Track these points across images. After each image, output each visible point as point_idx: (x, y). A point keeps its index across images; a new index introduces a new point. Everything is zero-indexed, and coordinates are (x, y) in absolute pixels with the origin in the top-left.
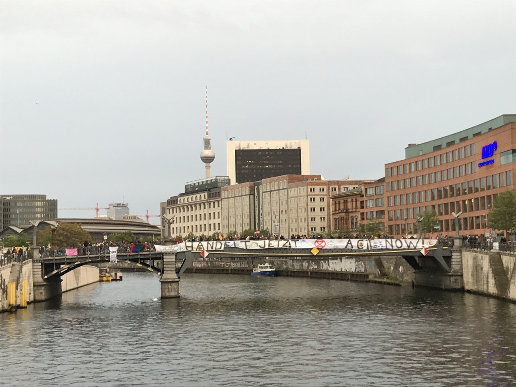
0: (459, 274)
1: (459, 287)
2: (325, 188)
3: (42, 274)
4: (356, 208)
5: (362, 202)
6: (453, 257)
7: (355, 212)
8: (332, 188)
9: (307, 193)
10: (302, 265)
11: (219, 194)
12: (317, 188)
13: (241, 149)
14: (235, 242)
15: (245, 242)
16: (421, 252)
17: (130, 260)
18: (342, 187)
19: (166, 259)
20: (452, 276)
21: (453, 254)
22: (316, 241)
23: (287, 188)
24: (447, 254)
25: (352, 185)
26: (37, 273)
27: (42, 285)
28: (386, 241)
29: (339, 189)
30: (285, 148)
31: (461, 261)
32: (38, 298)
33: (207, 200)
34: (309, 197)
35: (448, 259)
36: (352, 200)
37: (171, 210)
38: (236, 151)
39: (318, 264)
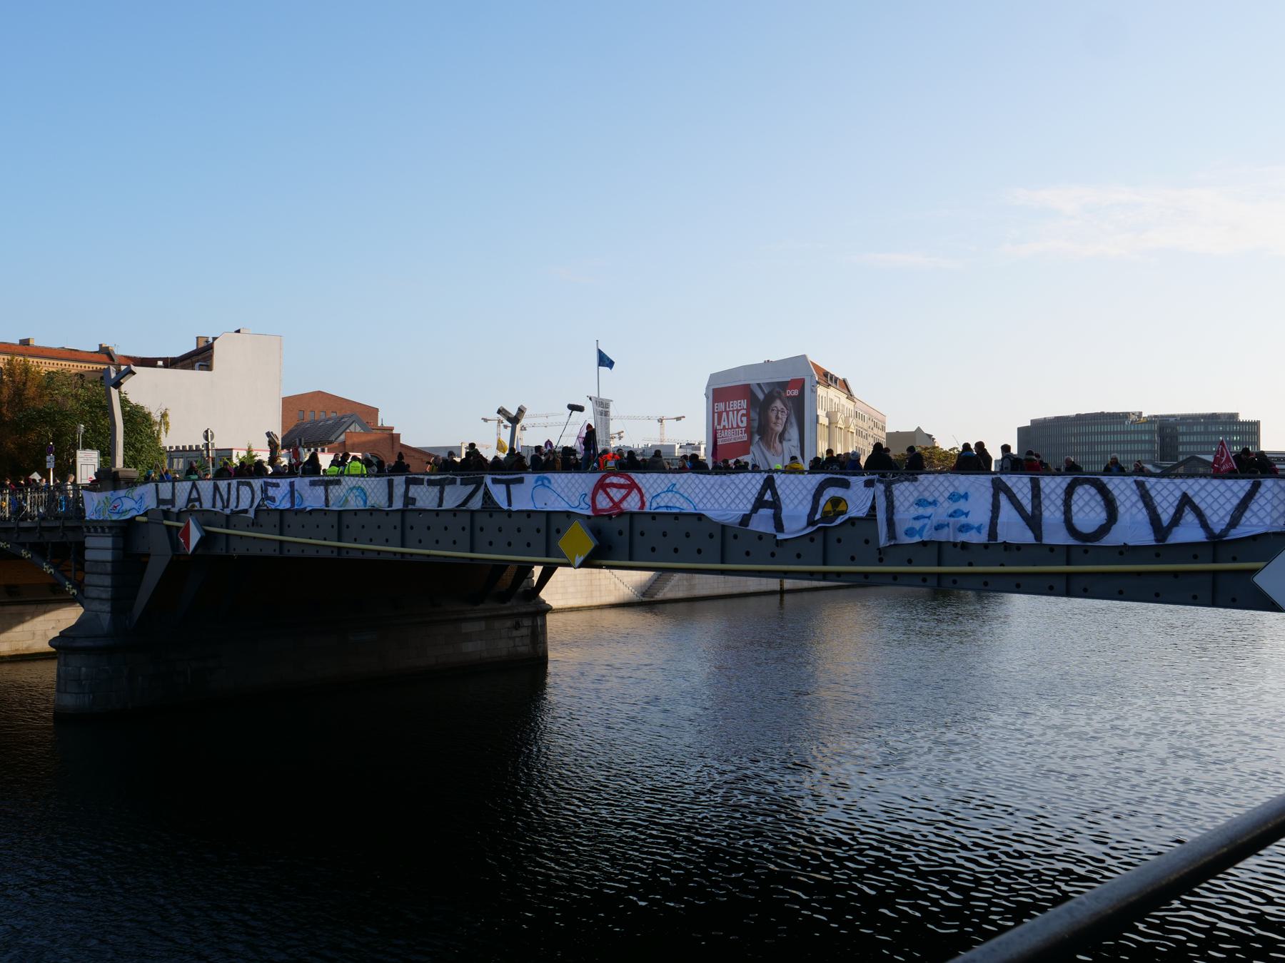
14: (292, 485)
16: (1259, 580)
22: (601, 486)
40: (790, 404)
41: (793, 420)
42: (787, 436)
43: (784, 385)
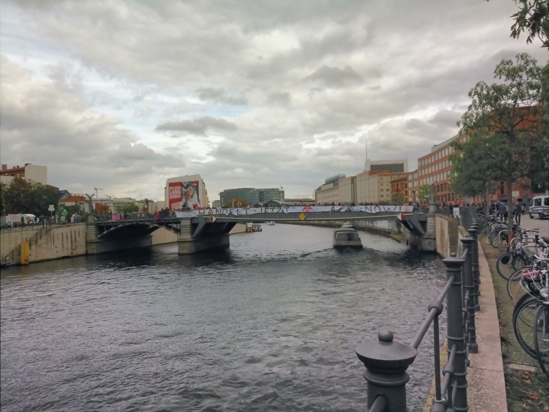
0: (432, 237)
1: (432, 249)
4: (403, 188)
5: (406, 184)
6: (428, 222)
10: (366, 224)
11: (337, 184)
15: (246, 209)
16: (398, 217)
19: (183, 223)
20: (426, 239)
21: (428, 219)
22: (305, 208)
24: (423, 219)
26: (90, 233)
28: (366, 207)
31: (435, 226)
32: (90, 251)
34: (380, 183)
35: (424, 224)
39: (372, 223)
40: (194, 188)
41: (195, 192)
42: (193, 196)
43: (192, 182)
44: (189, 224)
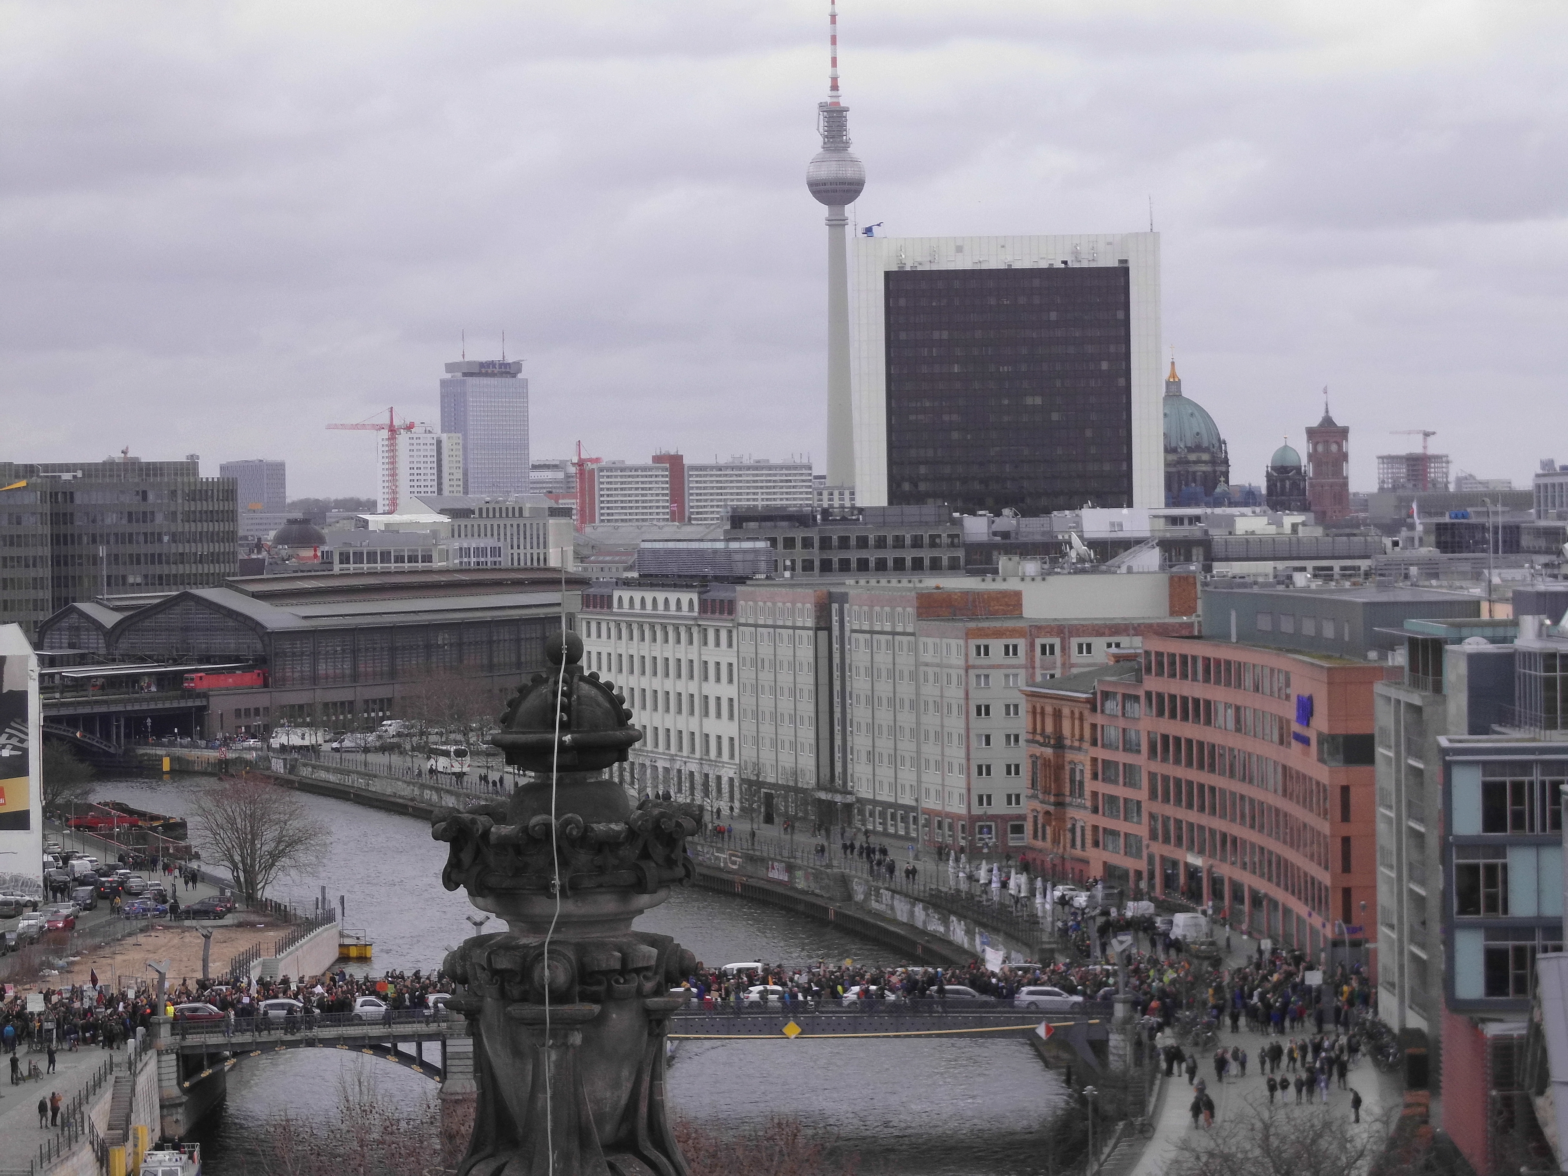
2: (1022, 644)
3: (178, 1077)
4: (1081, 739)
7: (1079, 749)
8: (1043, 647)
9: (967, 661)
12: (997, 646)
13: (908, 269)
17: (371, 1047)
18: (1074, 642)
23: (913, 634)
25: (1102, 634)
27: (180, 1105)
29: (1063, 649)
30: (1070, 265)
33: (695, 619)
36: (1072, 712)
37: (594, 626)
38: (887, 274)
44: (471, 1049)
